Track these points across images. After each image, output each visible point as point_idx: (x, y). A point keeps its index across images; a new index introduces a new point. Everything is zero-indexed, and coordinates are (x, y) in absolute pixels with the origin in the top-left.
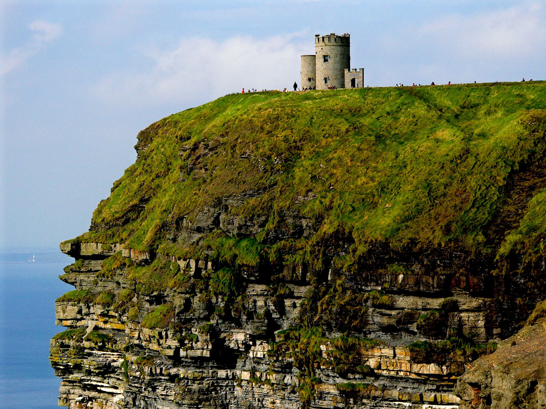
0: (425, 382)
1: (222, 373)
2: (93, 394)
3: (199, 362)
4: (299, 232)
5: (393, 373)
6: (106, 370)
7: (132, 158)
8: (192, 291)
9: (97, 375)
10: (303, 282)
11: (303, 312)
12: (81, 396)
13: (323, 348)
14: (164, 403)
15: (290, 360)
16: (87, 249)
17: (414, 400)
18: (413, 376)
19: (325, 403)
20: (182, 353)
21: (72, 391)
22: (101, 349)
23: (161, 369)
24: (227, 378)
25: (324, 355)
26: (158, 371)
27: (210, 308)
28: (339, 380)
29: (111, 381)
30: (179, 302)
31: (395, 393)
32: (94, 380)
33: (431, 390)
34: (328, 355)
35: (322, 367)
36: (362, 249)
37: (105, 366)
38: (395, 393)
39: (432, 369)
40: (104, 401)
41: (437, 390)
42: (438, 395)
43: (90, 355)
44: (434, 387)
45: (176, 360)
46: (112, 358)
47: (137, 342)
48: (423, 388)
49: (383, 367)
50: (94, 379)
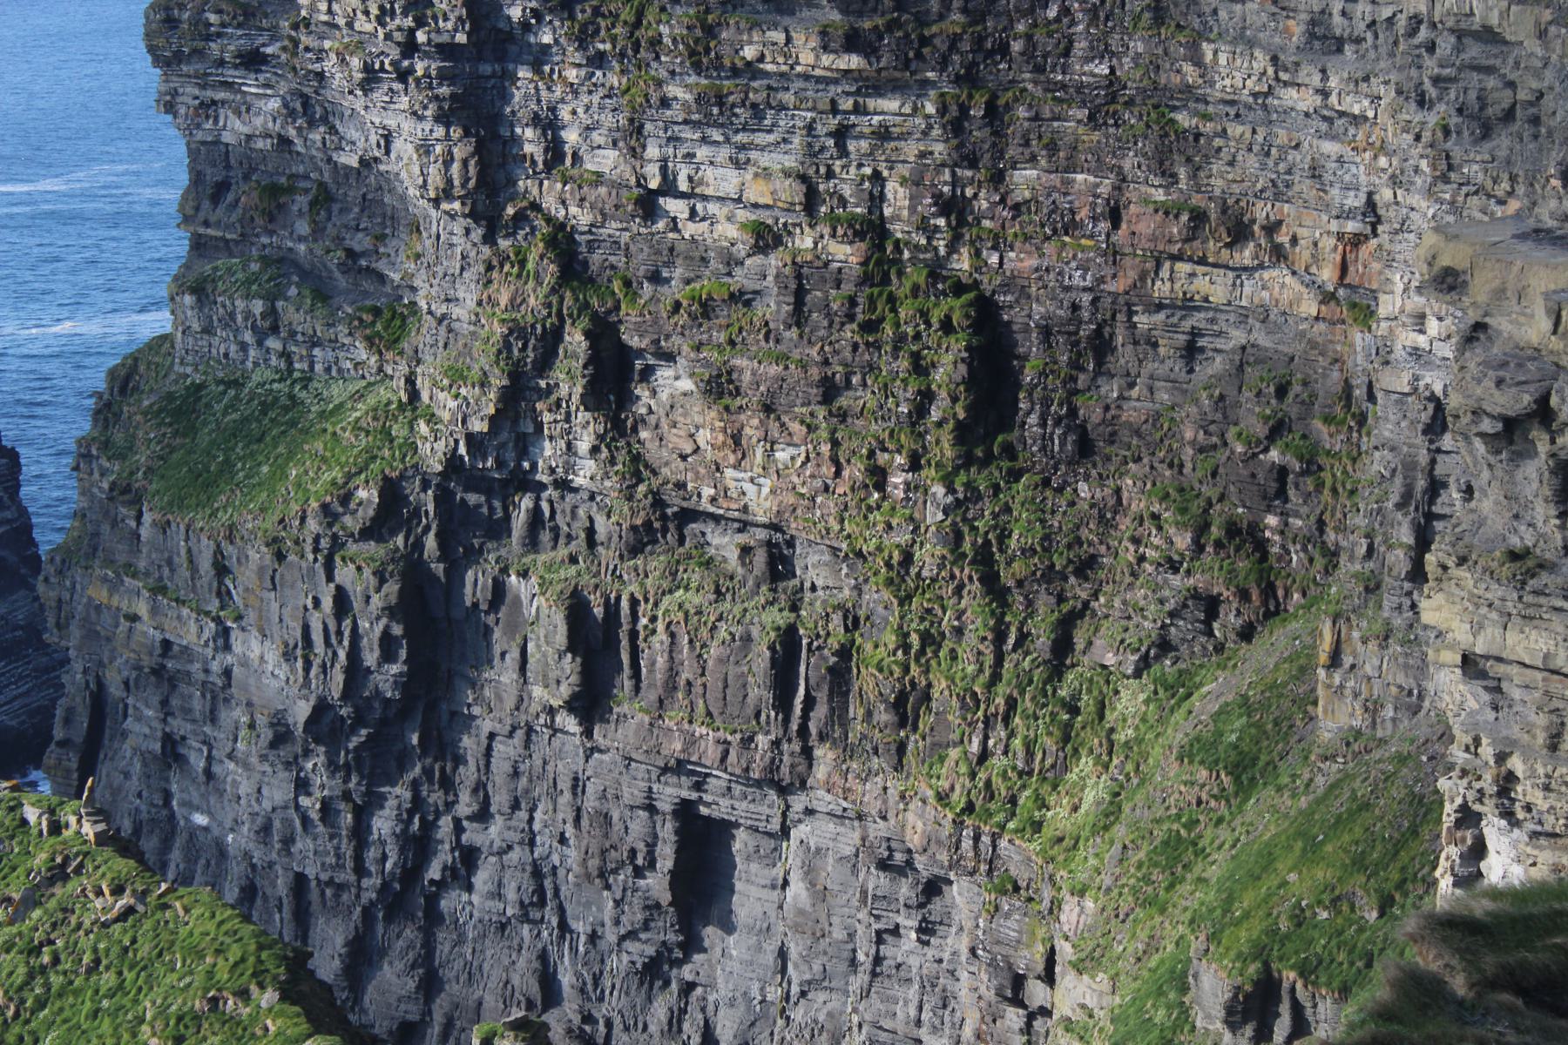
0: (836, 82)
1: (486, 69)
2: (221, 95)
3: (446, 50)
5: (784, 68)
9: (236, 67)
12: (196, 98)
13: (664, 29)
14: (384, 114)
15: (601, 46)
17: (821, 106)
18: (818, 72)
19: (669, 113)
20: (421, 37)
21: (181, 90)
22: (239, 26)
23: (382, 63)
24: (493, 75)
25: (667, 40)
26: (377, 66)
28: (692, 79)
29: (261, 77)
31: (788, 98)
32: (231, 74)
33: (848, 94)
34: (674, 40)
35: (663, 59)
37: (250, 52)
38: (788, 98)
39: (854, 61)
40: (243, 108)
41: (858, 92)
42: (861, 100)
43: (219, 35)
44: (853, 89)
46: (260, 41)
47: (325, 18)
48: (833, 90)
49: (768, 59)
50: (231, 72)
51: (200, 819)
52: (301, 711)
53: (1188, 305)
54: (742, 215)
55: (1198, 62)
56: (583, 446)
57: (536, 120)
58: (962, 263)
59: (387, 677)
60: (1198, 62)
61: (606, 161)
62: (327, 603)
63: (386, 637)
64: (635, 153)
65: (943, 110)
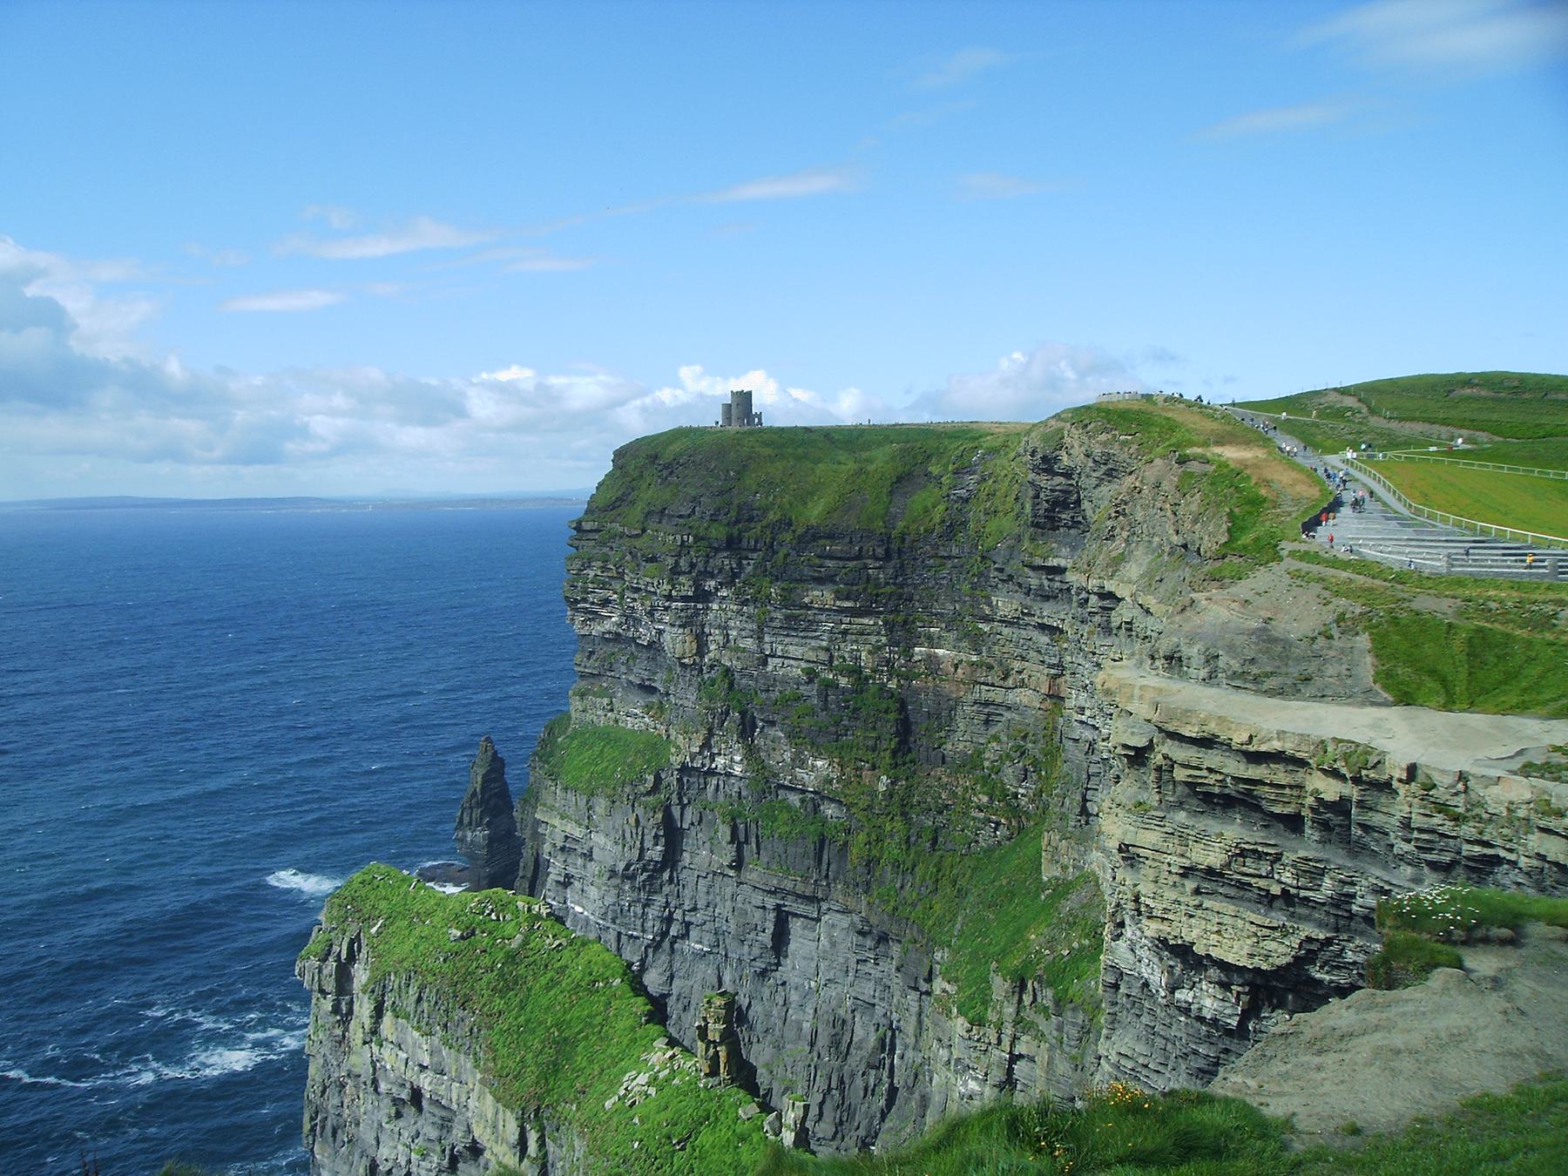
1: (700, 606)
3: (685, 599)
4: (751, 519)
6: (605, 602)
7: (609, 467)
8: (679, 555)
10: (755, 550)
11: (755, 568)
16: (587, 526)
27: (692, 566)
30: (670, 561)
36: (800, 531)
45: (669, 597)
51: (578, 909)
52: (621, 866)
53: (987, 704)
54: (804, 665)
55: (990, 605)
56: (737, 758)
57: (719, 627)
58: (892, 685)
59: (655, 853)
60: (990, 605)
61: (749, 643)
62: (632, 821)
63: (656, 837)
64: (760, 639)
65: (886, 623)
